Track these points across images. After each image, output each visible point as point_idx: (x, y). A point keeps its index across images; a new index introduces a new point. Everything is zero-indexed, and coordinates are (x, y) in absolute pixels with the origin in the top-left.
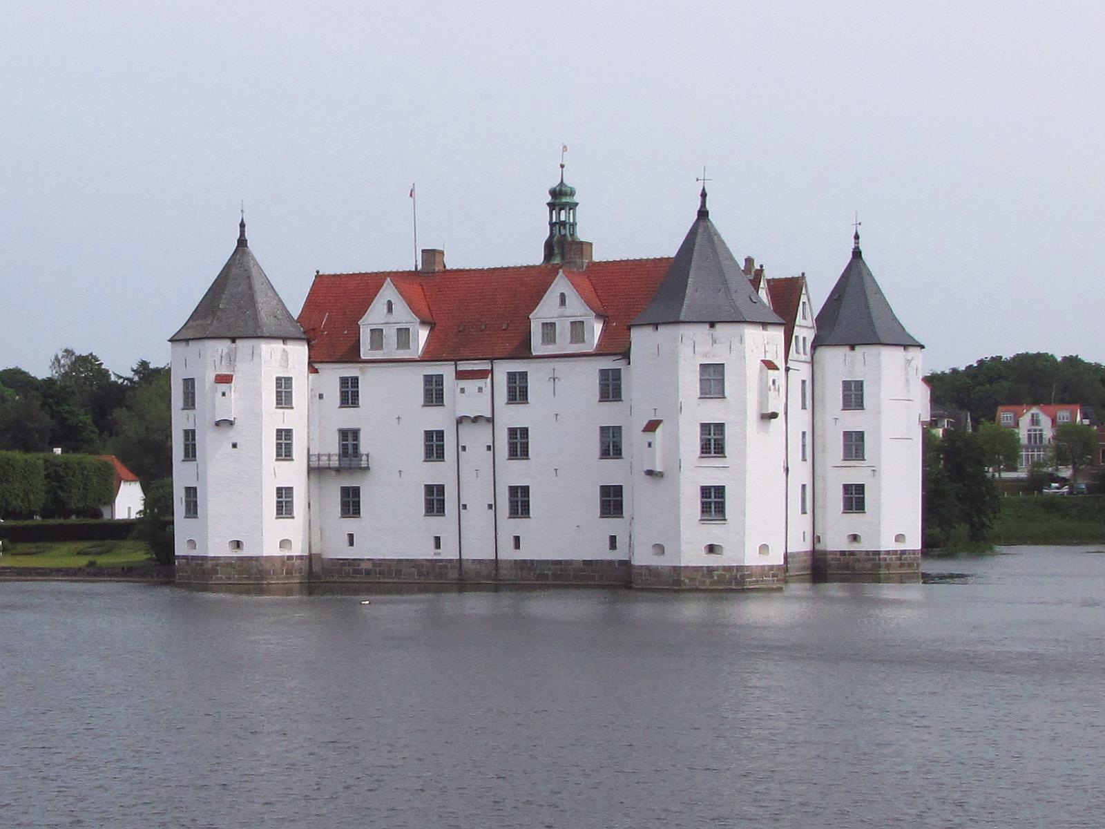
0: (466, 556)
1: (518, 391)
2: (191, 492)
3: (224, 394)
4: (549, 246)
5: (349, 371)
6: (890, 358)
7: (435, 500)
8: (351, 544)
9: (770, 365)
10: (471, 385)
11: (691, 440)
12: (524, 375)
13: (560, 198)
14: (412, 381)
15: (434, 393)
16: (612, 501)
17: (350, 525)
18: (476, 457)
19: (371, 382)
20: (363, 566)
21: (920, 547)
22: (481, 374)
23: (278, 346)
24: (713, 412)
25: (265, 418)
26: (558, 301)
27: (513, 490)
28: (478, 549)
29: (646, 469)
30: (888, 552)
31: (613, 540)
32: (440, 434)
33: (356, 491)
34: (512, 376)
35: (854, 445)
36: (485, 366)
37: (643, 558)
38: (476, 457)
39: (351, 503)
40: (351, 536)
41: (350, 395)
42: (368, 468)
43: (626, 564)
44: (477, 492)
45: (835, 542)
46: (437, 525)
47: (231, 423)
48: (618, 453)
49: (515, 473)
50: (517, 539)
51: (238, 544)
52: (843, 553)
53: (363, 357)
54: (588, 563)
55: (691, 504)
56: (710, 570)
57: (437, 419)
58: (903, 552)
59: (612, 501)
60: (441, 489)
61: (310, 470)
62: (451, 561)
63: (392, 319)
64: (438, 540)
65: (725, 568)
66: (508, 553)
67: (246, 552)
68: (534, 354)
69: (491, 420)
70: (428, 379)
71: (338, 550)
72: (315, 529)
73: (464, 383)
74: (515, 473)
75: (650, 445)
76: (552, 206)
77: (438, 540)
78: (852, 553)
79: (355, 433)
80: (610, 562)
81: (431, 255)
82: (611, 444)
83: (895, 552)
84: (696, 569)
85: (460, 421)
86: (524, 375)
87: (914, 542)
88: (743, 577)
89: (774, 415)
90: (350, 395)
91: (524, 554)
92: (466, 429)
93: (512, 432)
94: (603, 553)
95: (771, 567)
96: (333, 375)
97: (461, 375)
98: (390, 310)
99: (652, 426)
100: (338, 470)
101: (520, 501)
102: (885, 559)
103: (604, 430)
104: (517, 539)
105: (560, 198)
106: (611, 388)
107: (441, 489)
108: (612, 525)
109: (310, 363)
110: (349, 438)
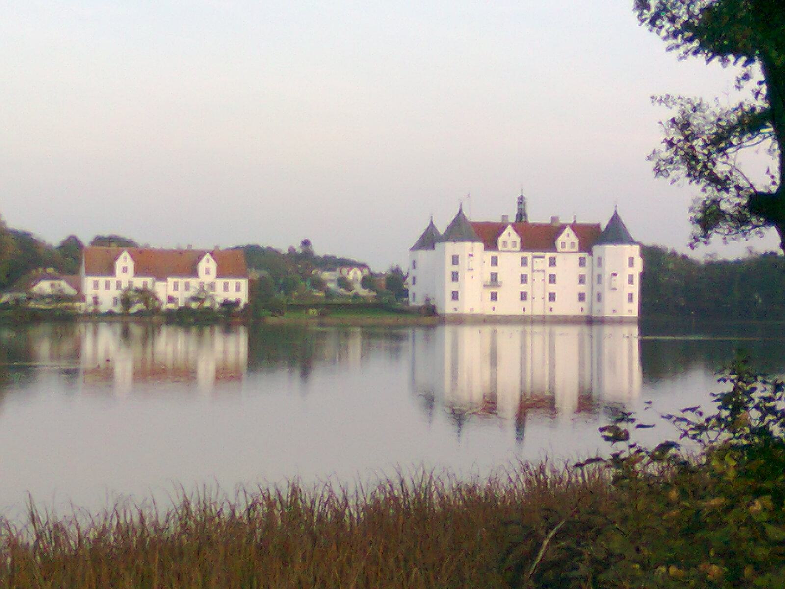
1: (553, 262)
5: (494, 254)
7: (524, 296)
13: (521, 201)
15: (524, 262)
17: (494, 303)
19: (502, 258)
22: (543, 257)
28: (538, 311)
31: (582, 309)
34: (551, 258)
36: (542, 254)
39: (494, 297)
41: (494, 261)
46: (524, 304)
47: (473, 270)
49: (551, 288)
51: (456, 309)
57: (526, 270)
60: (526, 293)
66: (548, 313)
70: (522, 258)
71: (489, 312)
74: (551, 288)
90: (494, 261)
91: (553, 313)
101: (552, 297)
104: (551, 309)
105: (521, 201)
106: (582, 262)
107: (526, 293)
110: (494, 277)
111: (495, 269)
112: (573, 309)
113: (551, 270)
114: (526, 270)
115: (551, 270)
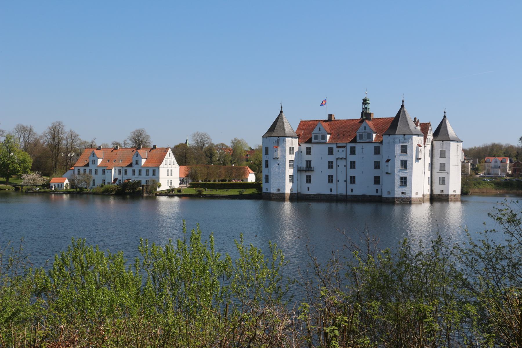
0: (338, 193)
1: (353, 151)
2: (267, 176)
3: (276, 151)
4: (362, 114)
6: (453, 145)
7: (330, 179)
8: (309, 190)
9: (420, 146)
10: (341, 150)
11: (398, 165)
12: (354, 147)
14: (325, 148)
15: (331, 151)
16: (377, 180)
17: (308, 185)
18: (341, 168)
20: (312, 196)
21: (460, 194)
23: (290, 139)
24: (404, 158)
25: (287, 158)
26: (364, 128)
27: (351, 177)
29: (386, 172)
30: (451, 195)
31: (377, 190)
32: (332, 162)
33: (310, 176)
35: (443, 167)
37: (385, 195)
38: (341, 168)
39: (309, 180)
40: (308, 188)
42: (313, 171)
43: (380, 197)
44: (342, 177)
45: (437, 192)
48: (379, 168)
49: (351, 173)
50: (352, 190)
51: (279, 190)
52: (439, 195)
53: (312, 142)
54: (370, 196)
55: (398, 182)
56: (402, 198)
57: (332, 158)
58: (455, 195)
59: (377, 180)
60: (332, 176)
61: (298, 170)
62: (334, 195)
63: (320, 132)
64: (331, 189)
65: (406, 198)
66: (349, 193)
67: (281, 192)
68: (357, 142)
69: (346, 159)
72: (299, 186)
73: (339, 149)
74: (351, 173)
75: (387, 166)
76: (363, 103)
77: (331, 189)
78: (441, 195)
79: (310, 161)
80: (376, 196)
81: (330, 116)
82: (377, 165)
83: (453, 195)
84: (399, 198)
85: (337, 159)
86: (354, 147)
87: (459, 192)
88: (411, 200)
89: (420, 159)
91: (354, 193)
92: (339, 161)
93: (351, 162)
94: (375, 194)
95: (419, 198)
96: (304, 146)
97: (338, 147)
98: (320, 130)
99: (388, 161)
100: (305, 171)
101: (353, 180)
102: (450, 197)
103: (375, 161)
104: (352, 190)
106: (377, 151)
107: (332, 176)
108: (377, 186)
109: (298, 144)
111: (308, 157)
112: (370, 190)
113: (351, 158)
114: (332, 158)
115: (351, 158)
